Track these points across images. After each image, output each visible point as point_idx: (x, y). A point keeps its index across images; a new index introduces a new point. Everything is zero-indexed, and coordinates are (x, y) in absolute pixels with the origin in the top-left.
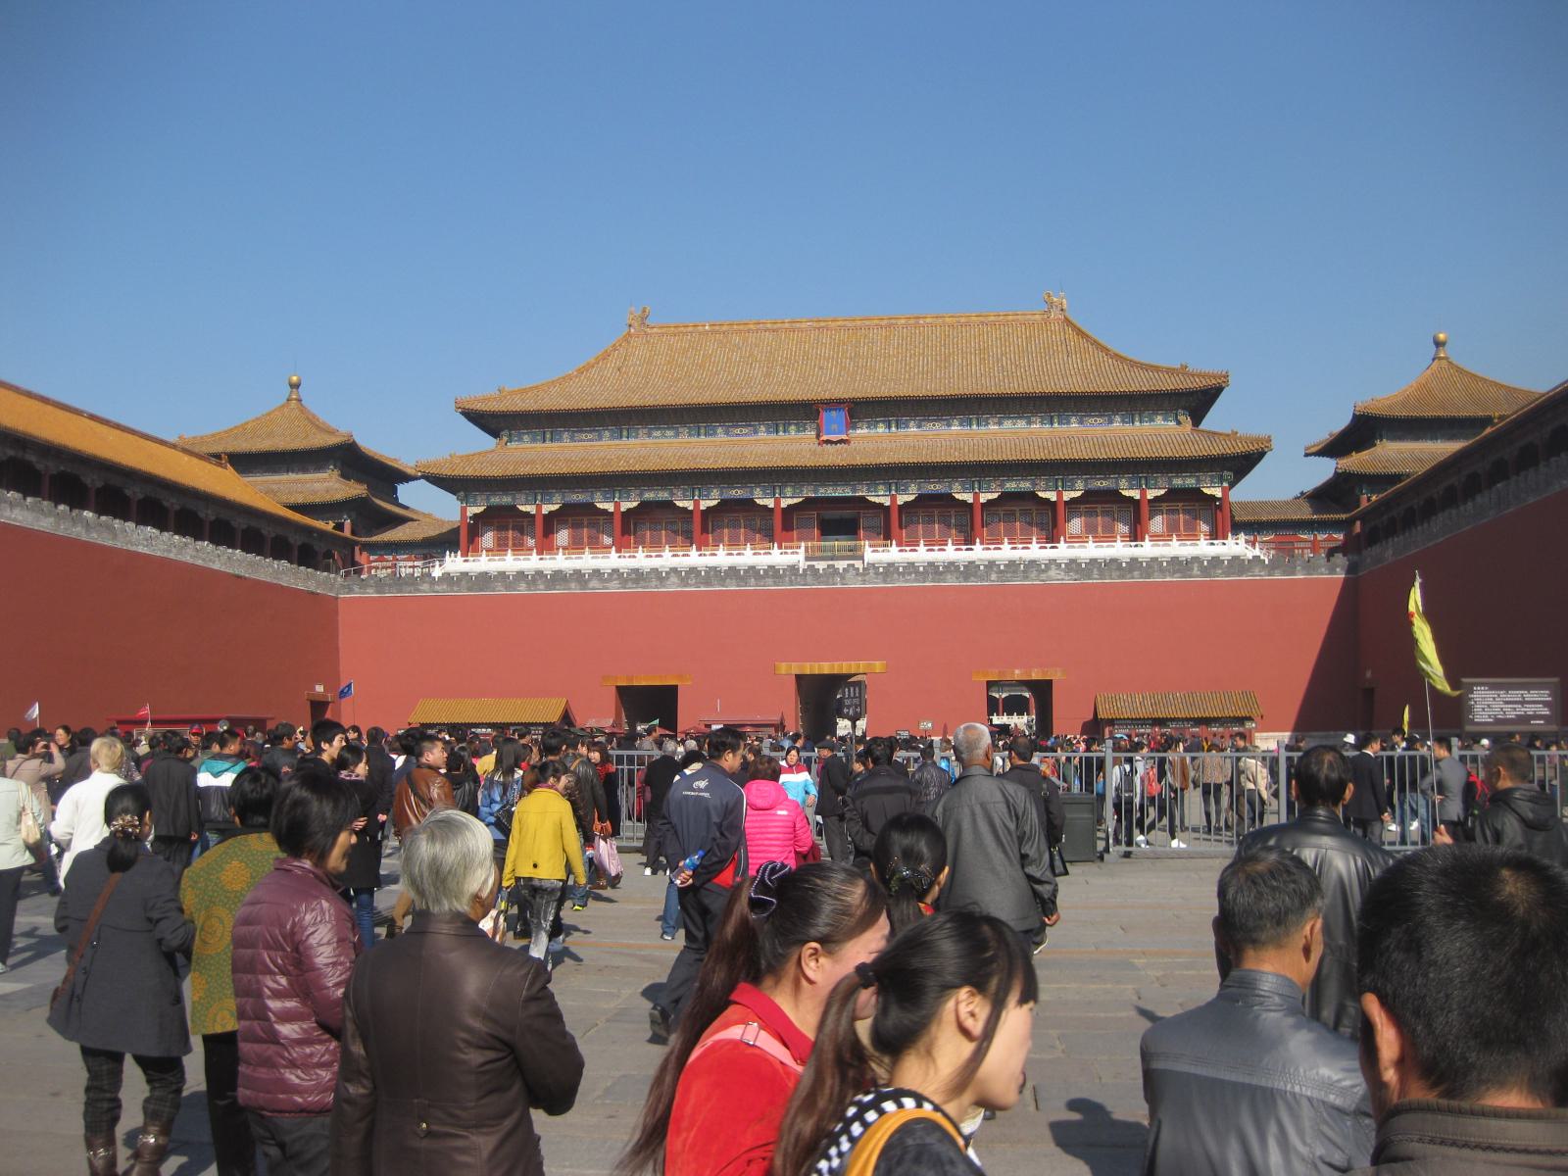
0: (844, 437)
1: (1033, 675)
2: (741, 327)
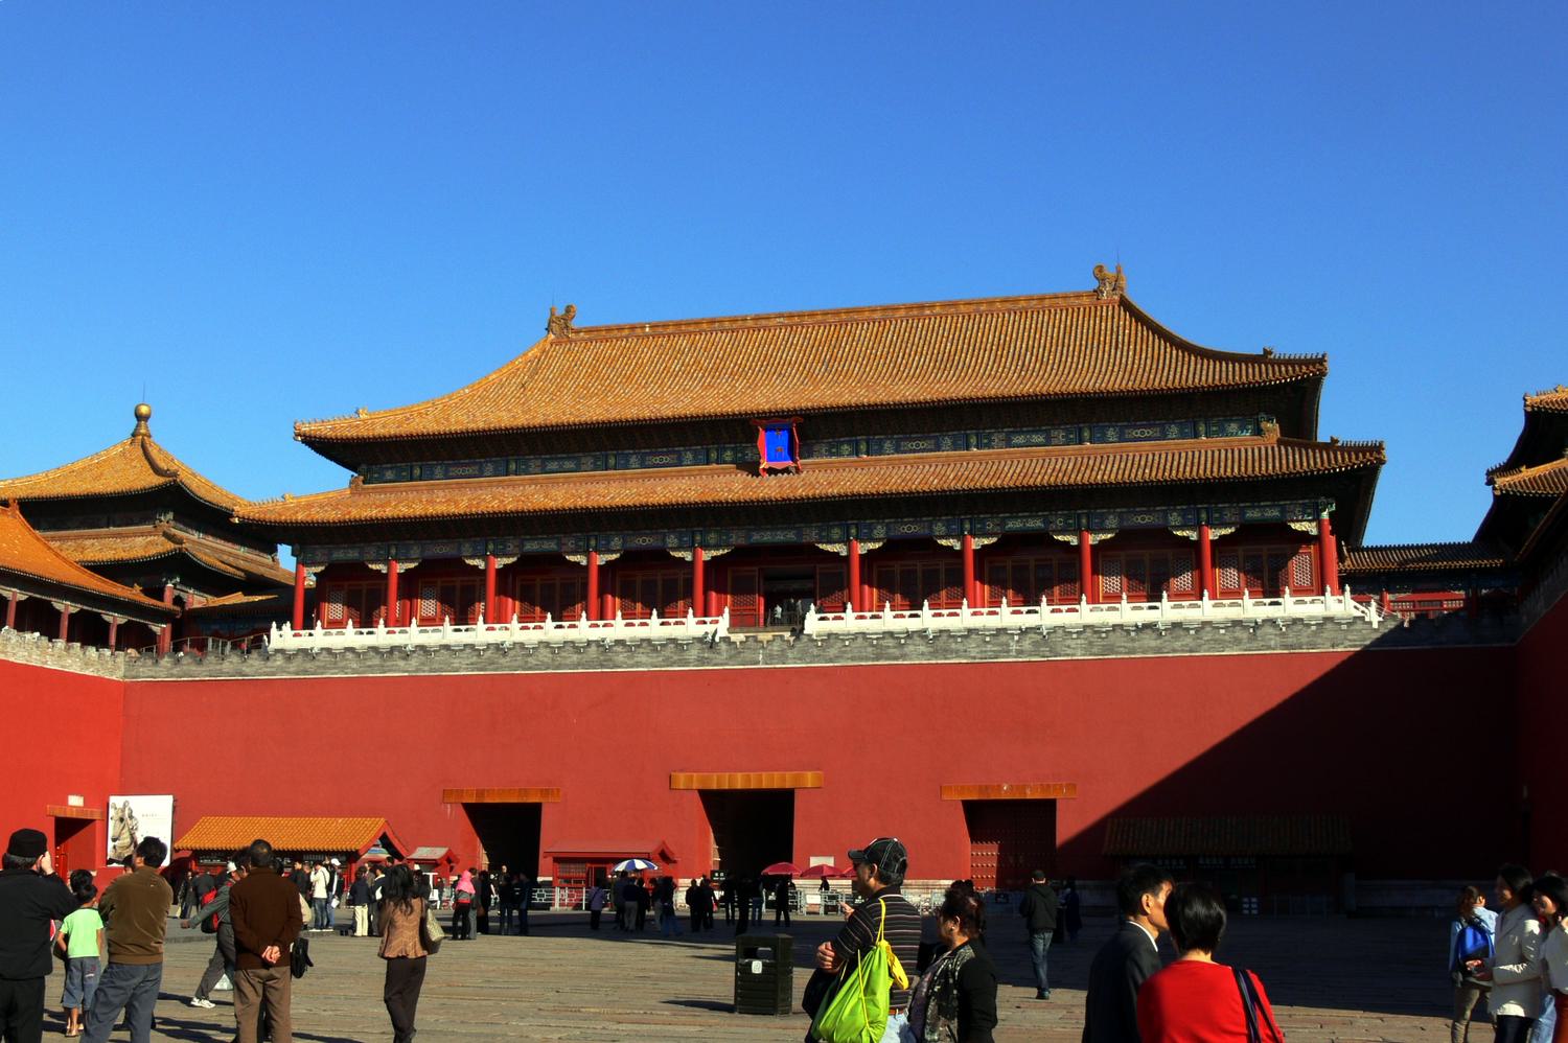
1: (1028, 792)
2: (691, 329)
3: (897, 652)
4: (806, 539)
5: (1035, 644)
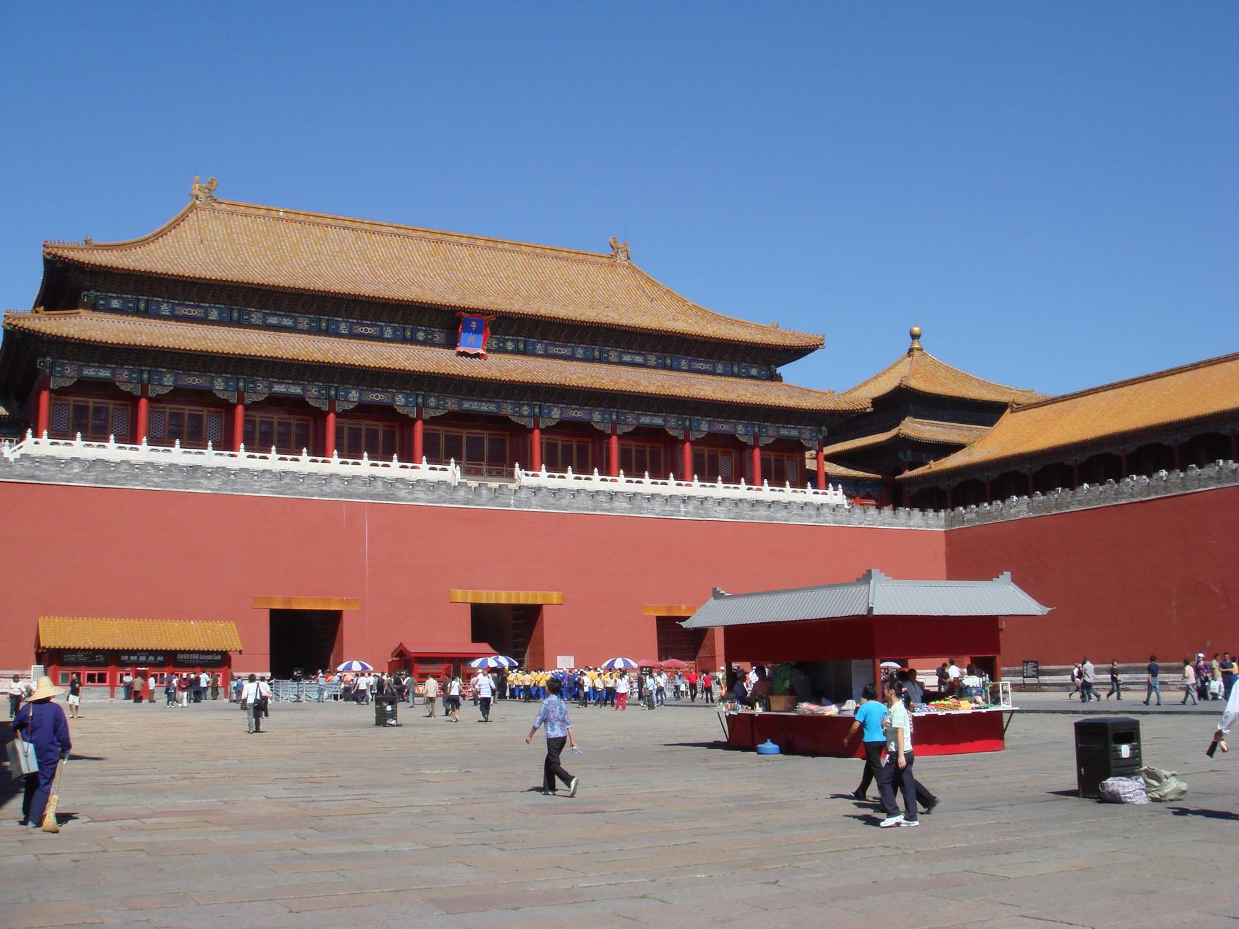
0: (481, 351)
3: (607, 506)
4: (504, 412)
5: (696, 508)
